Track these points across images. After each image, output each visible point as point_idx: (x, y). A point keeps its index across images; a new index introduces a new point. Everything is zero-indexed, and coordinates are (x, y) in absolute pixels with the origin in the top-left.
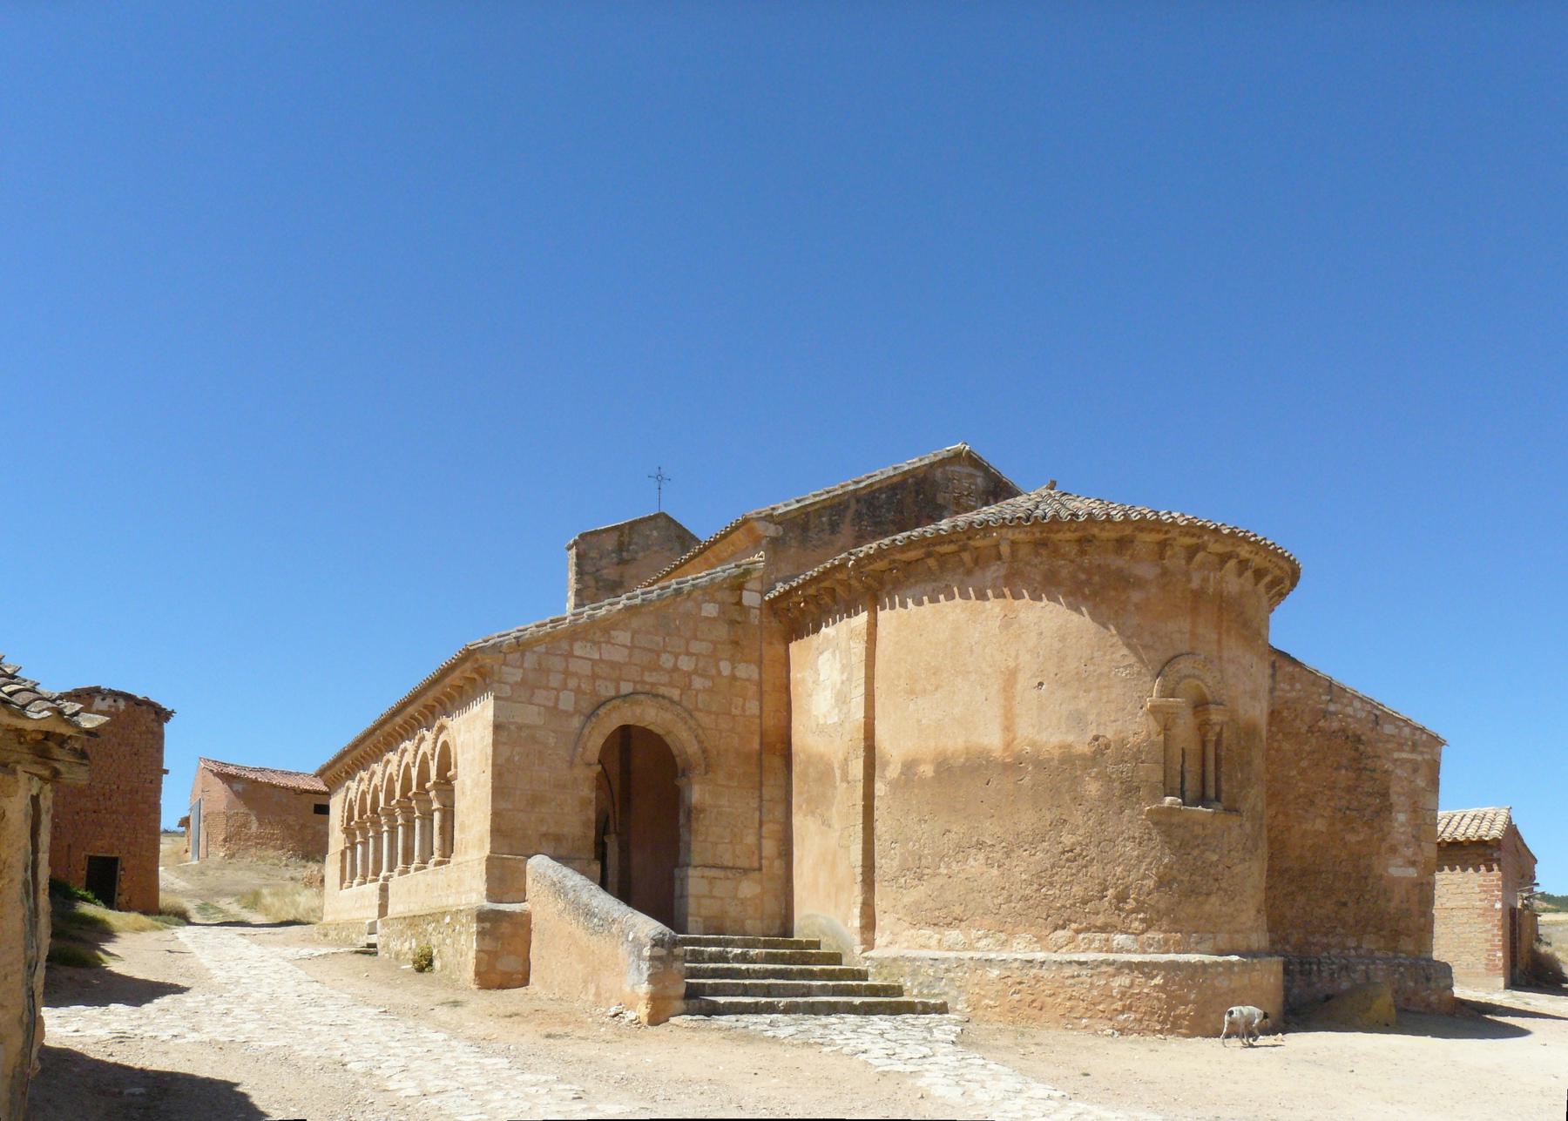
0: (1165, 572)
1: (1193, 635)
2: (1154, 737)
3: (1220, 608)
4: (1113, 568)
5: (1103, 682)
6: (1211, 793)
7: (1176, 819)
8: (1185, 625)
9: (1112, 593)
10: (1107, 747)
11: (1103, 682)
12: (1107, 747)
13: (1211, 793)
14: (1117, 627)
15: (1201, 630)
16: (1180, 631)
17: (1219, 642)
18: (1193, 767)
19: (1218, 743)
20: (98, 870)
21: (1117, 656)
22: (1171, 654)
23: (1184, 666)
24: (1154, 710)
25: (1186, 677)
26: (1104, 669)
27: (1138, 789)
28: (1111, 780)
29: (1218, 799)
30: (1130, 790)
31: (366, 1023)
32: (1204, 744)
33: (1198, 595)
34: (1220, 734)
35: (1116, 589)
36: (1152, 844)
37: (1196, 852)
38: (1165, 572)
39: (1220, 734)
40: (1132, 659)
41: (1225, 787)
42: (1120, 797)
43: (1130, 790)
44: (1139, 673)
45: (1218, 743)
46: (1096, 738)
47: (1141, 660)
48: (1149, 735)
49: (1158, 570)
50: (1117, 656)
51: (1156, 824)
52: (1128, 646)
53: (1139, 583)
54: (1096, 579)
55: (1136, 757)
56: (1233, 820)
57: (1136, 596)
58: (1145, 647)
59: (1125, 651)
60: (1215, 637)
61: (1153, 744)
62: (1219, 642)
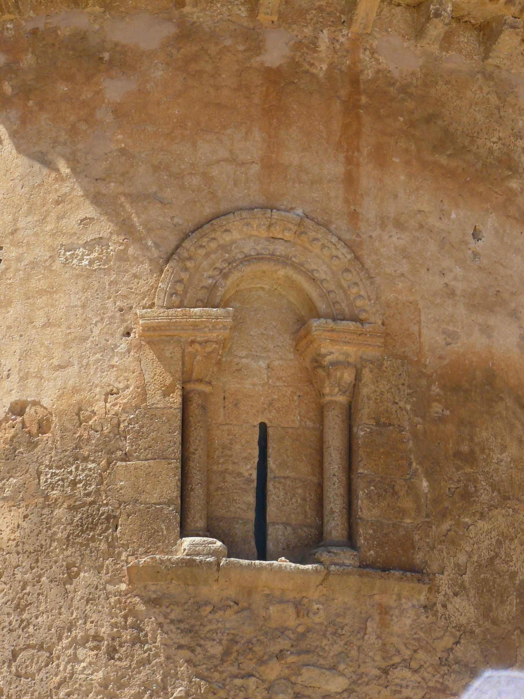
0: (187, 33)
1: (270, 166)
2: (155, 399)
3: (351, 108)
4: (64, 32)
5: (38, 283)
6: (335, 527)
7: (212, 591)
8: (250, 145)
9: (63, 88)
10: (43, 426)
11: (38, 283)
12: (43, 426)
13: (335, 527)
14: (73, 161)
15: (291, 157)
16: (233, 160)
17: (350, 181)
18: (287, 469)
19: (350, 413)
20: (107, 7)
21: (72, 222)
22: (208, 211)
23: (242, 236)
24: (156, 337)
25: (248, 259)
26: (41, 253)
27: (112, 520)
28: (50, 504)
29: (351, 541)
30: (93, 524)
31: (332, 450)
32: (321, 411)
33: (277, 80)
34: (355, 388)
35: (69, 78)
36: (139, 653)
37: (273, 671)
38: (187, 33)
39: (355, 388)
40: (105, 228)
41: (366, 510)
42: (68, 541)
43: (93, 524)
44: (122, 257)
45: (350, 413)
46: (18, 409)
47: (126, 228)
48: (143, 395)
49: (170, 30)
50: (72, 222)
51: (153, 602)
52: (96, 199)
53: (123, 60)
54: (28, 60)
55: (113, 445)
56: (404, 598)
57: (115, 89)
58: (135, 198)
59: (89, 210)
60: (335, 168)
61: (151, 413)
62: (350, 181)
